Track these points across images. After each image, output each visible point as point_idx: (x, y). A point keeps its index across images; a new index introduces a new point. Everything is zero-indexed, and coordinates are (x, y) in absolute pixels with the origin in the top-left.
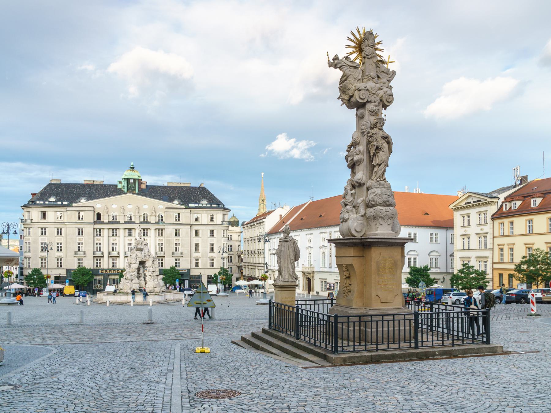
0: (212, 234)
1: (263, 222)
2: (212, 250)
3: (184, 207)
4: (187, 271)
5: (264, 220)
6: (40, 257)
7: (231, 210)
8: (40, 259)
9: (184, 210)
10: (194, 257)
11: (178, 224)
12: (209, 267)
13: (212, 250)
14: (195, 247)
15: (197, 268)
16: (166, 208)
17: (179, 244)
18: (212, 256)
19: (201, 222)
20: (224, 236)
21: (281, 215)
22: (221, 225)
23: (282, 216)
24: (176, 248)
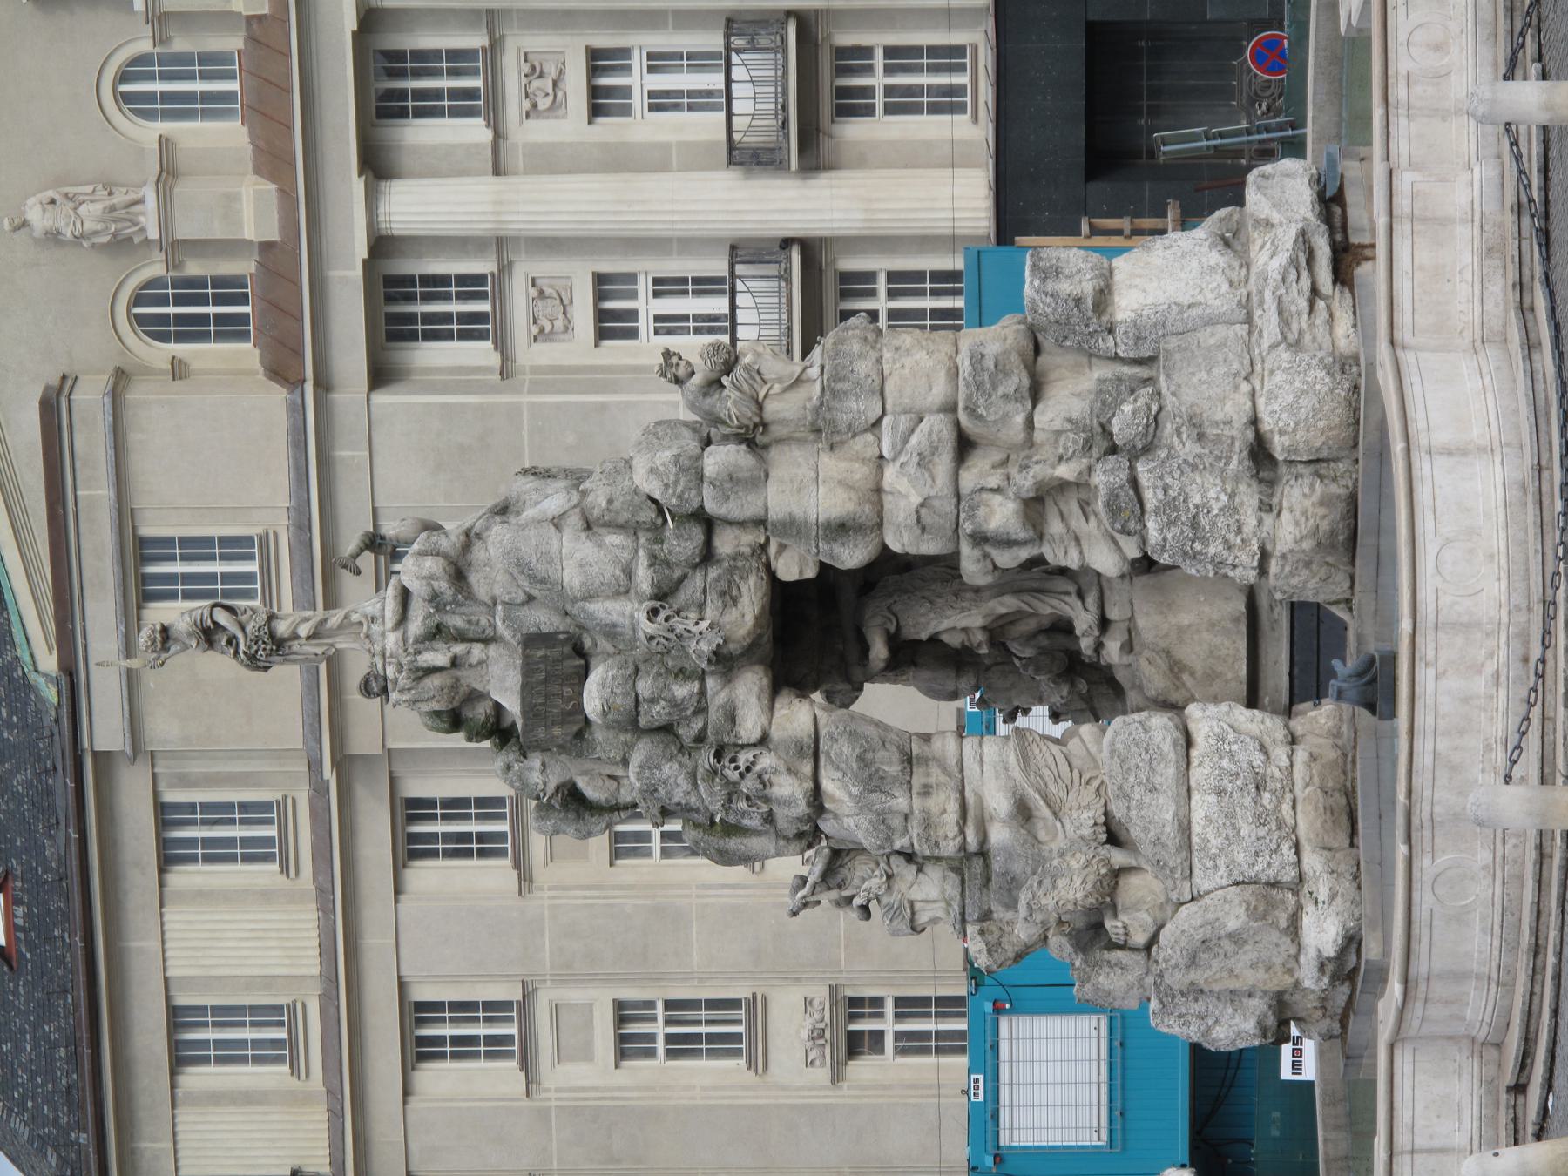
6: (822, 1074)
8: (864, 1068)
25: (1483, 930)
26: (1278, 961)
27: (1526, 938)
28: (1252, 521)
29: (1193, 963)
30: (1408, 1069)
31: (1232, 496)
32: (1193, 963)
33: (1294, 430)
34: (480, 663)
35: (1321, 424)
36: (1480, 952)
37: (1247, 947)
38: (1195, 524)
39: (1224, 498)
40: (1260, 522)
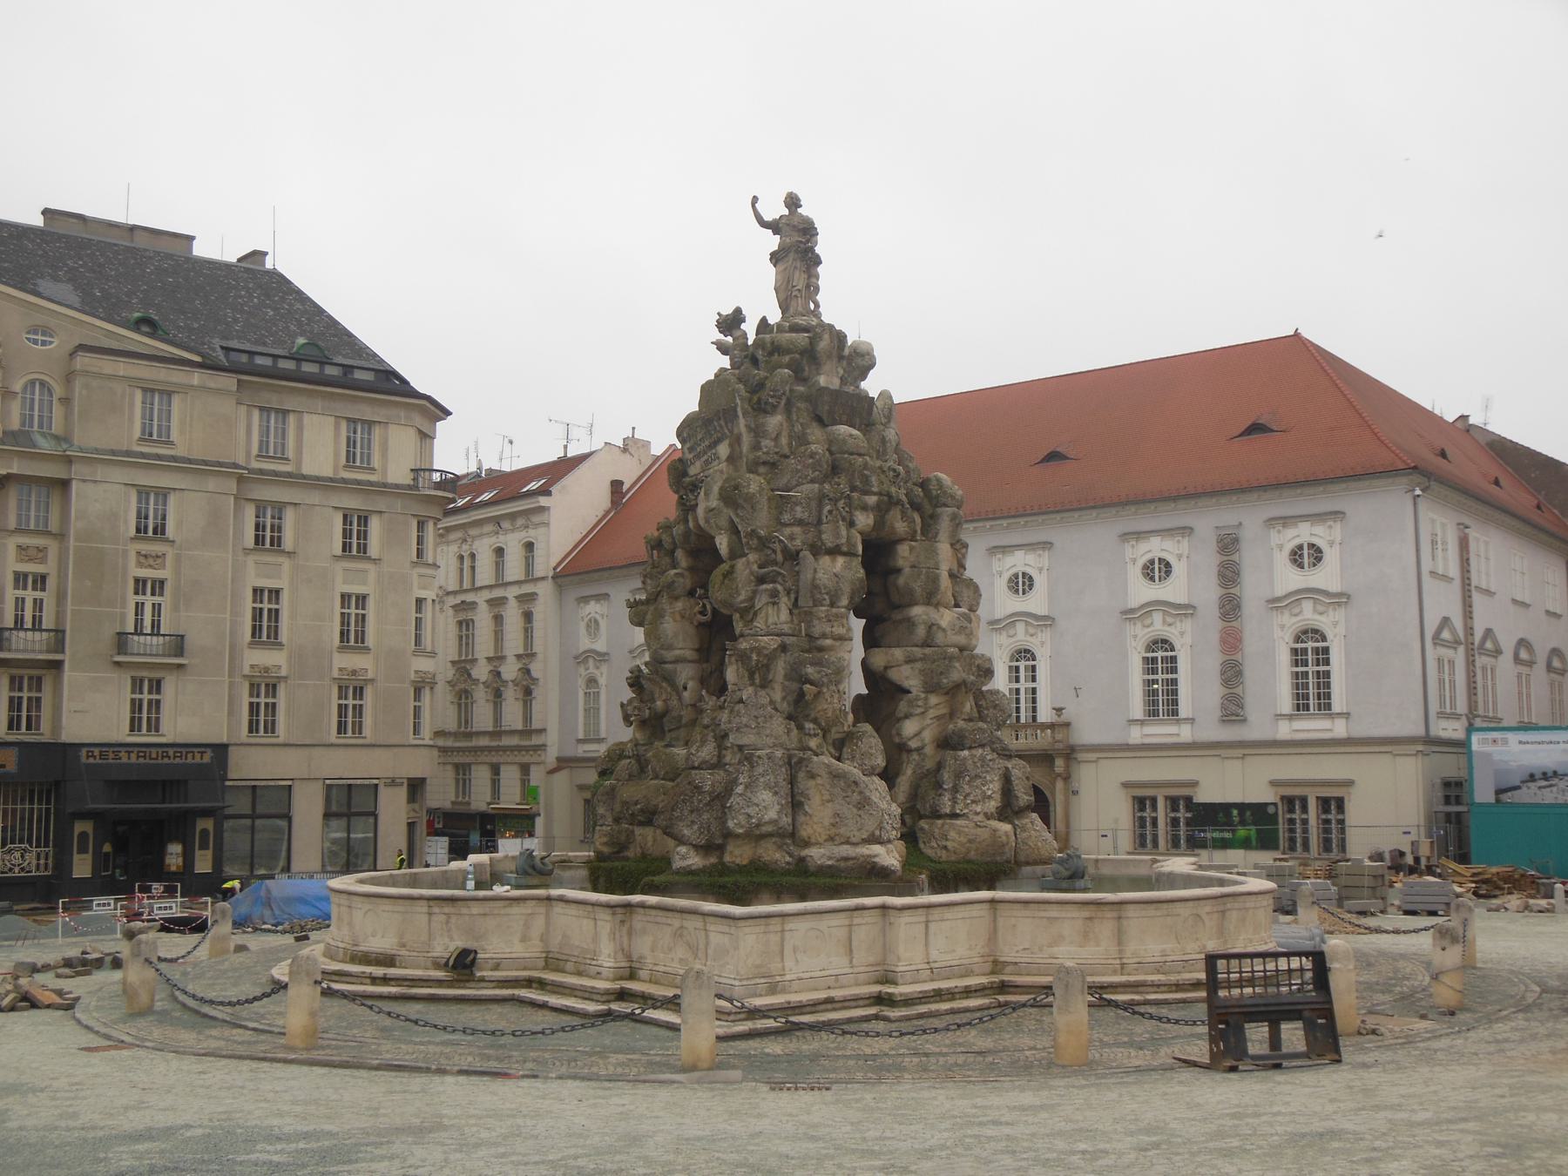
0: (355, 544)
1: (542, 509)
2: (352, 635)
3: (197, 359)
4: (207, 758)
5: (543, 501)
7: (448, 413)
9: (197, 378)
10: (247, 671)
11: (159, 457)
12: (333, 737)
13: (352, 635)
14: (257, 614)
15: (261, 737)
16: (82, 348)
17: (159, 586)
18: (354, 672)
19: (299, 462)
20: (420, 553)
21: (616, 485)
22: (409, 487)
23: (625, 488)
24: (139, 608)
25: (1164, 951)
26: (842, 830)
27: (837, 994)
28: (979, 809)
29: (835, 776)
30: (975, 914)
31: (990, 797)
32: (835, 776)
33: (1035, 830)
34: (838, 373)
35: (1039, 844)
36: (1145, 950)
37: (855, 810)
38: (977, 776)
39: (989, 793)
40: (977, 814)
